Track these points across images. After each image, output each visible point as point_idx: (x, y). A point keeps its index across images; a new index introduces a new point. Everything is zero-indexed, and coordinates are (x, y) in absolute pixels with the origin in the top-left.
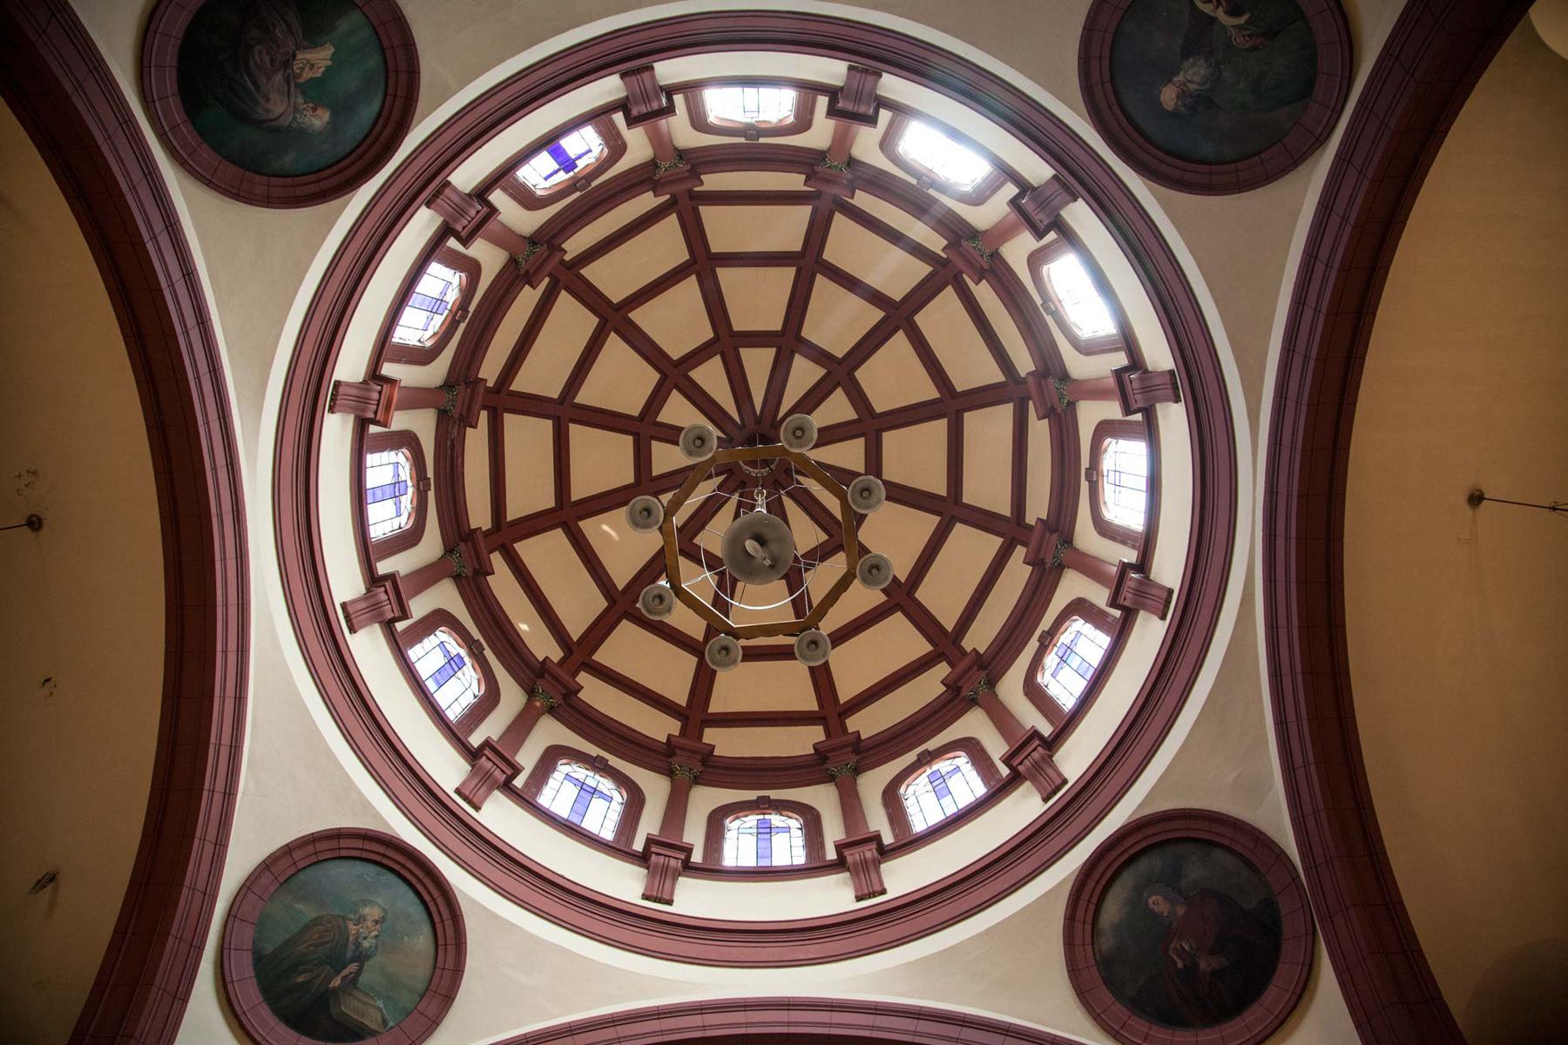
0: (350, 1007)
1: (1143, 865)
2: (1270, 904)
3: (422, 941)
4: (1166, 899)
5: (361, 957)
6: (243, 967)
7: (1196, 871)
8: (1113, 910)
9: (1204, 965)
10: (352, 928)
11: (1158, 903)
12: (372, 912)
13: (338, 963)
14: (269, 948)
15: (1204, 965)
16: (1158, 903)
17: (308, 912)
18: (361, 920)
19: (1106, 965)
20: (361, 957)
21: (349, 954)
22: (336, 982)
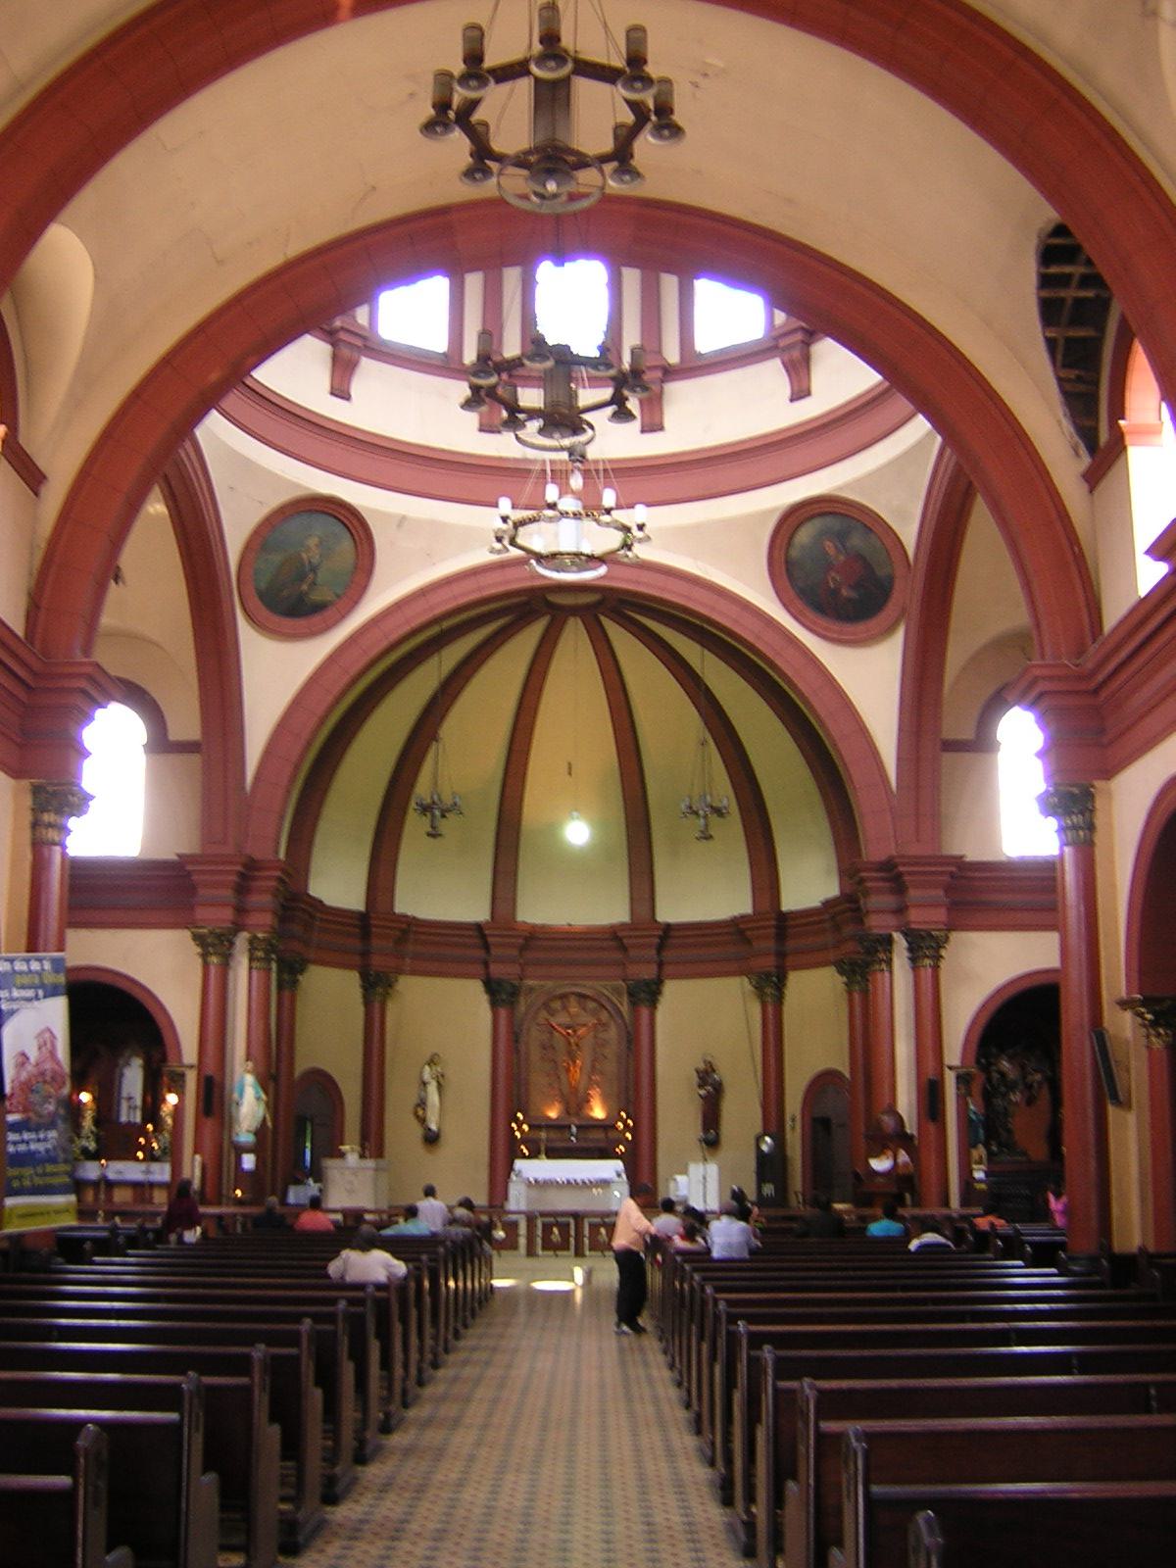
0: (316, 596)
1: (829, 521)
2: (891, 579)
3: (347, 544)
4: (836, 547)
5: (314, 569)
6: (255, 602)
7: (856, 541)
8: (805, 535)
9: (845, 592)
10: (304, 556)
11: (829, 546)
12: (312, 542)
13: (302, 578)
14: (263, 585)
15: (845, 592)
16: (829, 546)
17: (277, 558)
18: (308, 549)
19: (789, 564)
20: (314, 569)
21: (307, 570)
22: (305, 587)
